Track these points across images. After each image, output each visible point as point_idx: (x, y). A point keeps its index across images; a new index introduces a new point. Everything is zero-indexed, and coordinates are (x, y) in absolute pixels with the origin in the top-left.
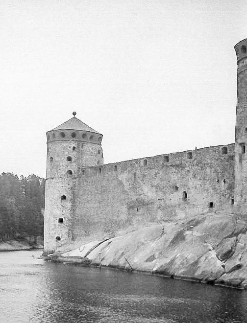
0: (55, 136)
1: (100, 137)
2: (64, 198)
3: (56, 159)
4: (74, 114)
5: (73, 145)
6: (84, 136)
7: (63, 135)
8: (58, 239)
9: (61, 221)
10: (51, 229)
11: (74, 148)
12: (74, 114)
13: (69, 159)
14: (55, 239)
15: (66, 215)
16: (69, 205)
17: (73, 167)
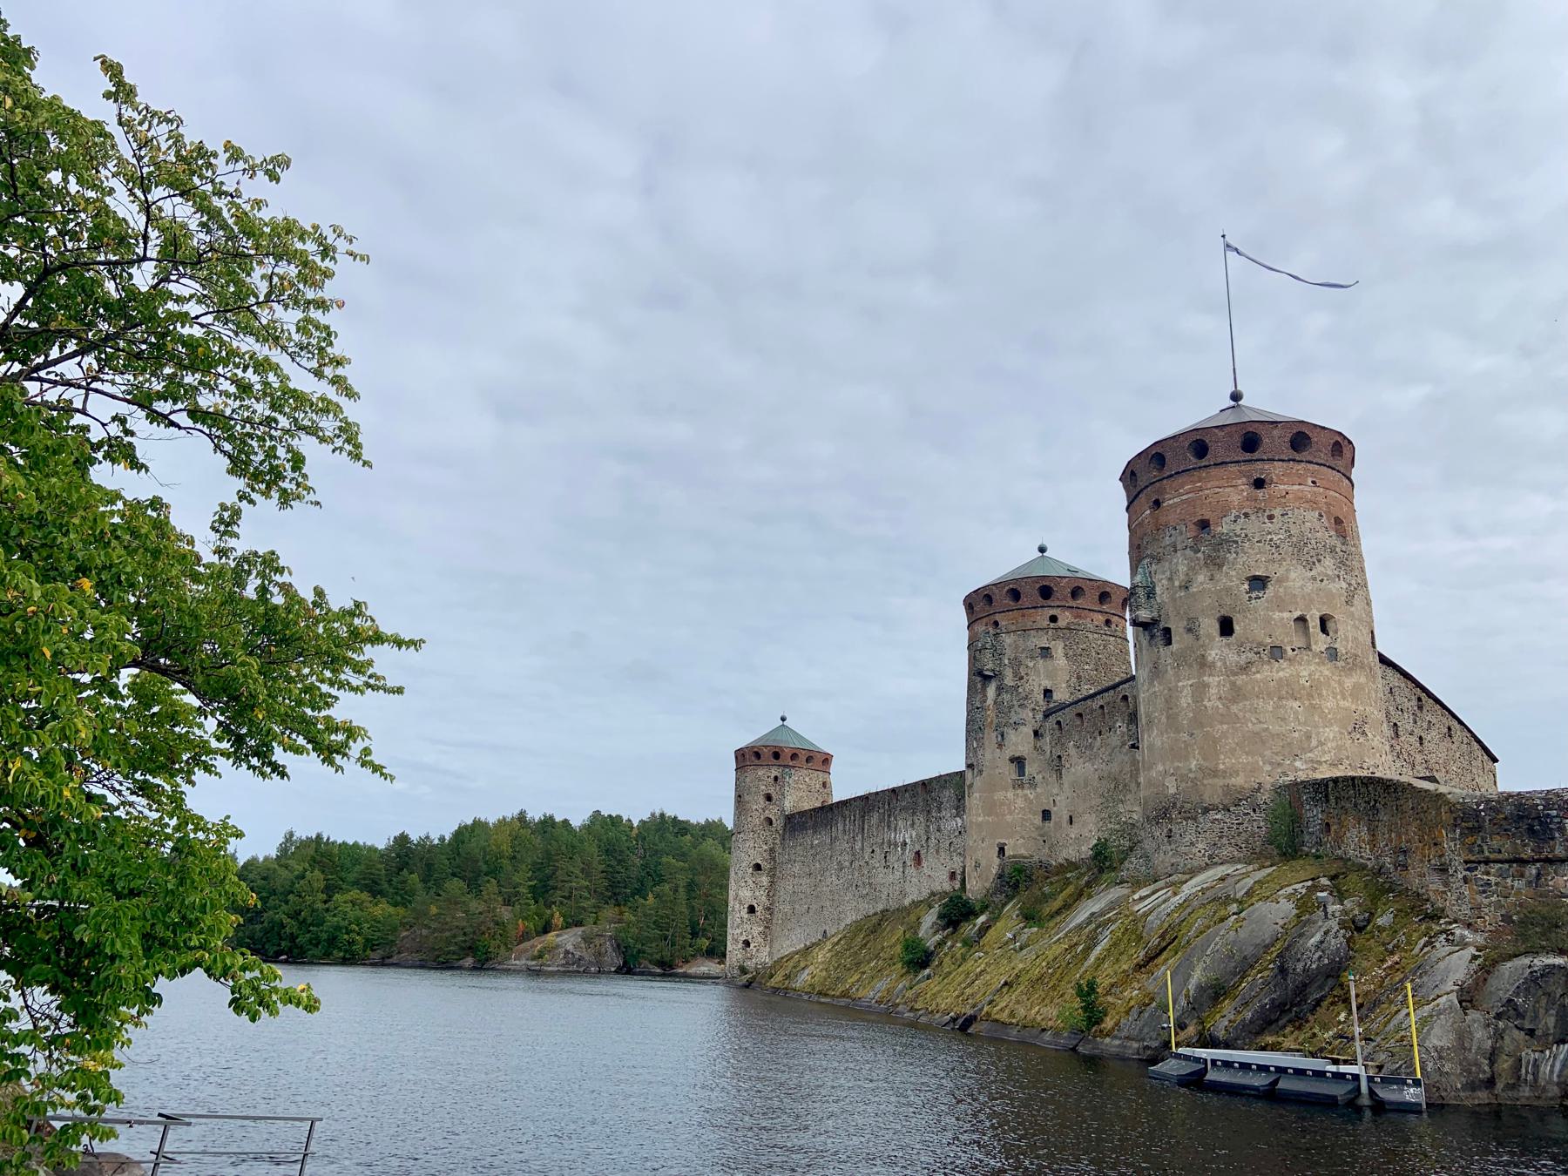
0: (748, 758)
1: (827, 760)
2: (758, 867)
3: (747, 798)
4: (783, 719)
5: (774, 772)
6: (794, 756)
7: (758, 755)
8: (747, 944)
9: (752, 910)
10: (738, 927)
11: (776, 778)
12: (783, 719)
13: (769, 798)
14: (740, 945)
15: (761, 900)
16: (765, 880)
17: (773, 812)
